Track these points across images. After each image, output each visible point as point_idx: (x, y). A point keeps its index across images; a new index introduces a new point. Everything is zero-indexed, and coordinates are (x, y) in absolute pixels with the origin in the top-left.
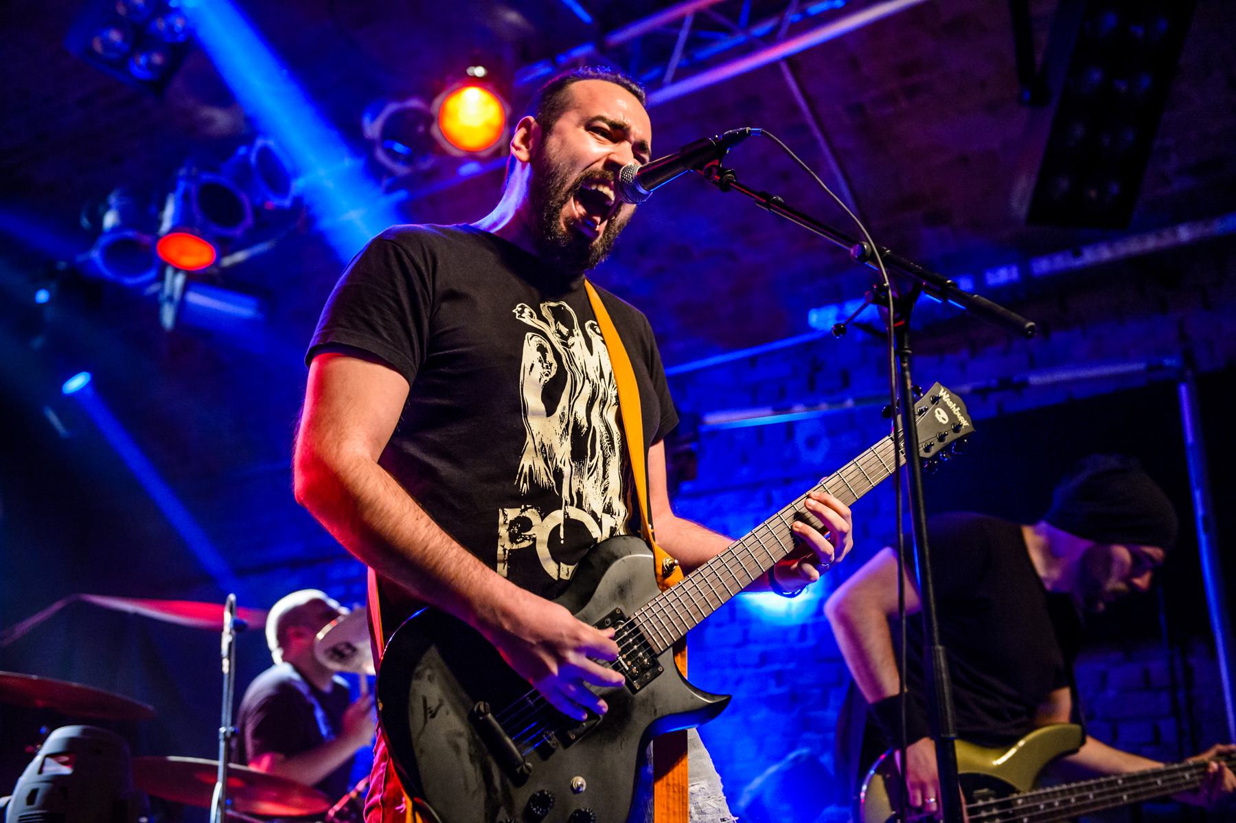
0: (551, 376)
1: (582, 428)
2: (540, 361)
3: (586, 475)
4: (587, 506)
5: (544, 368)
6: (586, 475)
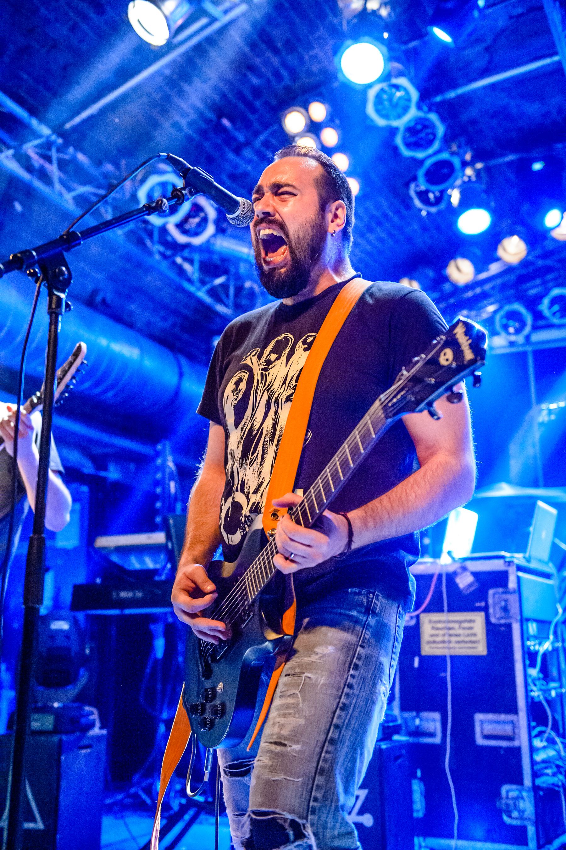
0: (238, 400)
1: (253, 432)
2: (233, 392)
3: (248, 467)
4: (248, 488)
5: (234, 395)
6: (248, 467)
